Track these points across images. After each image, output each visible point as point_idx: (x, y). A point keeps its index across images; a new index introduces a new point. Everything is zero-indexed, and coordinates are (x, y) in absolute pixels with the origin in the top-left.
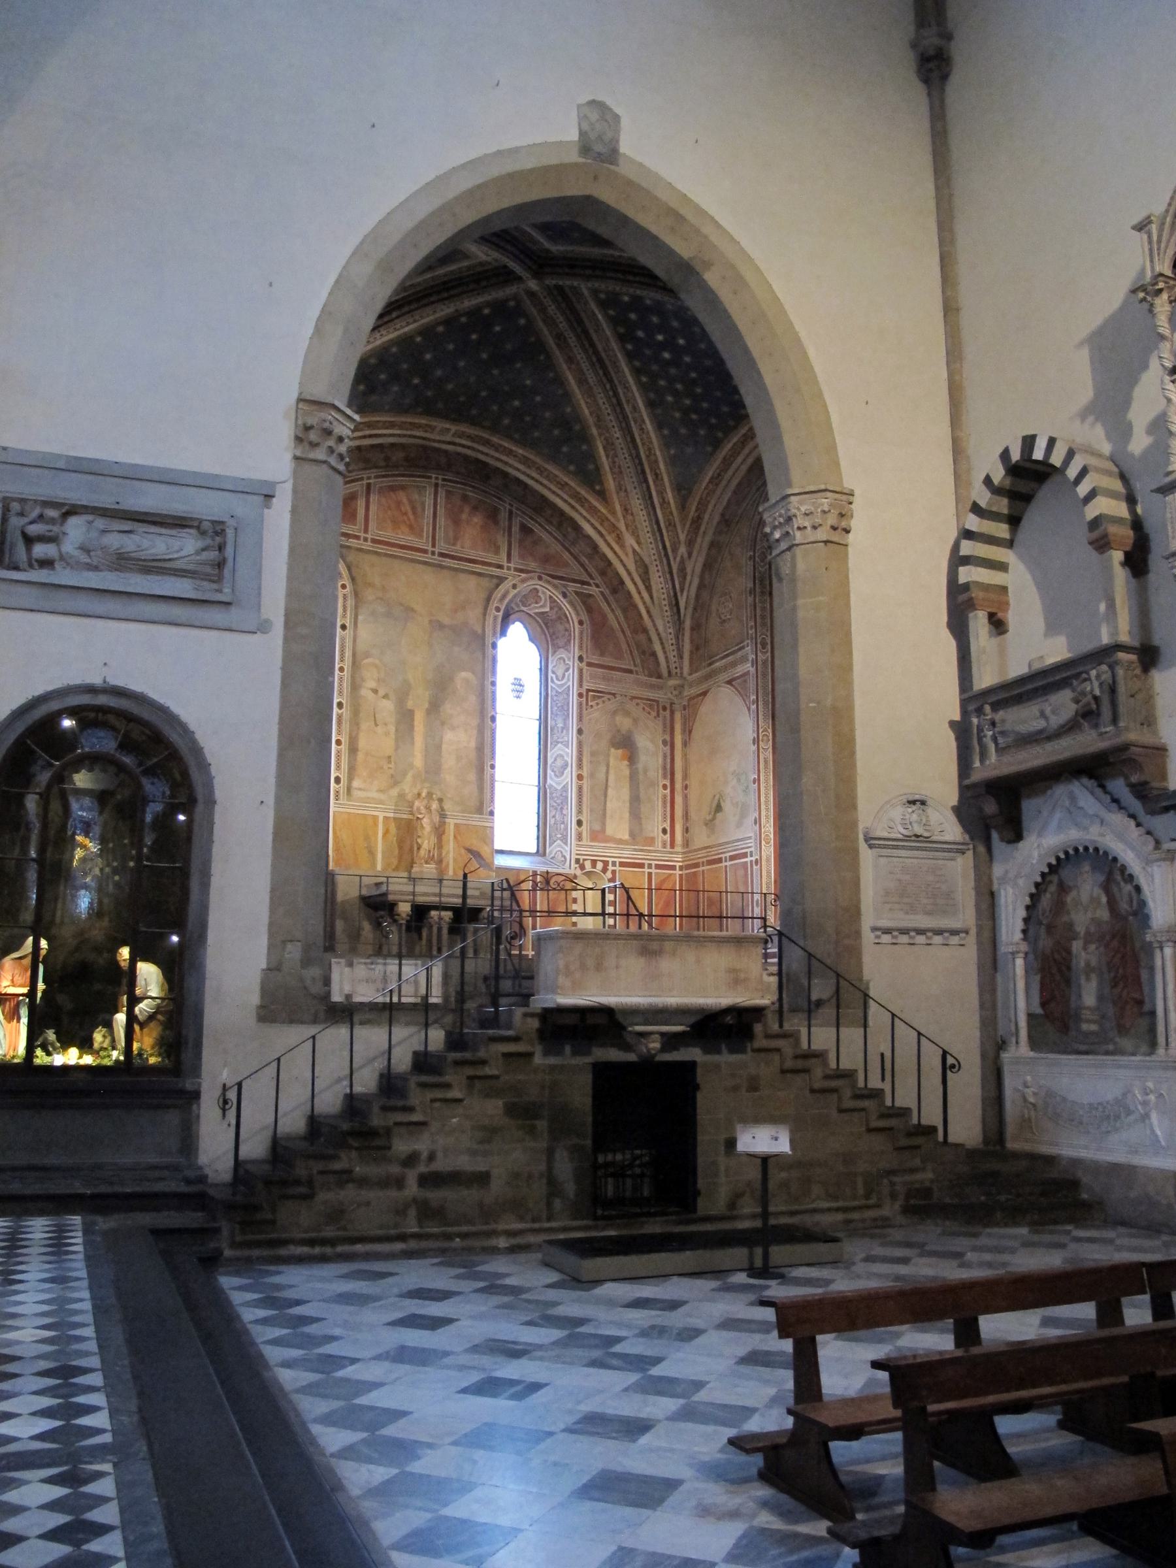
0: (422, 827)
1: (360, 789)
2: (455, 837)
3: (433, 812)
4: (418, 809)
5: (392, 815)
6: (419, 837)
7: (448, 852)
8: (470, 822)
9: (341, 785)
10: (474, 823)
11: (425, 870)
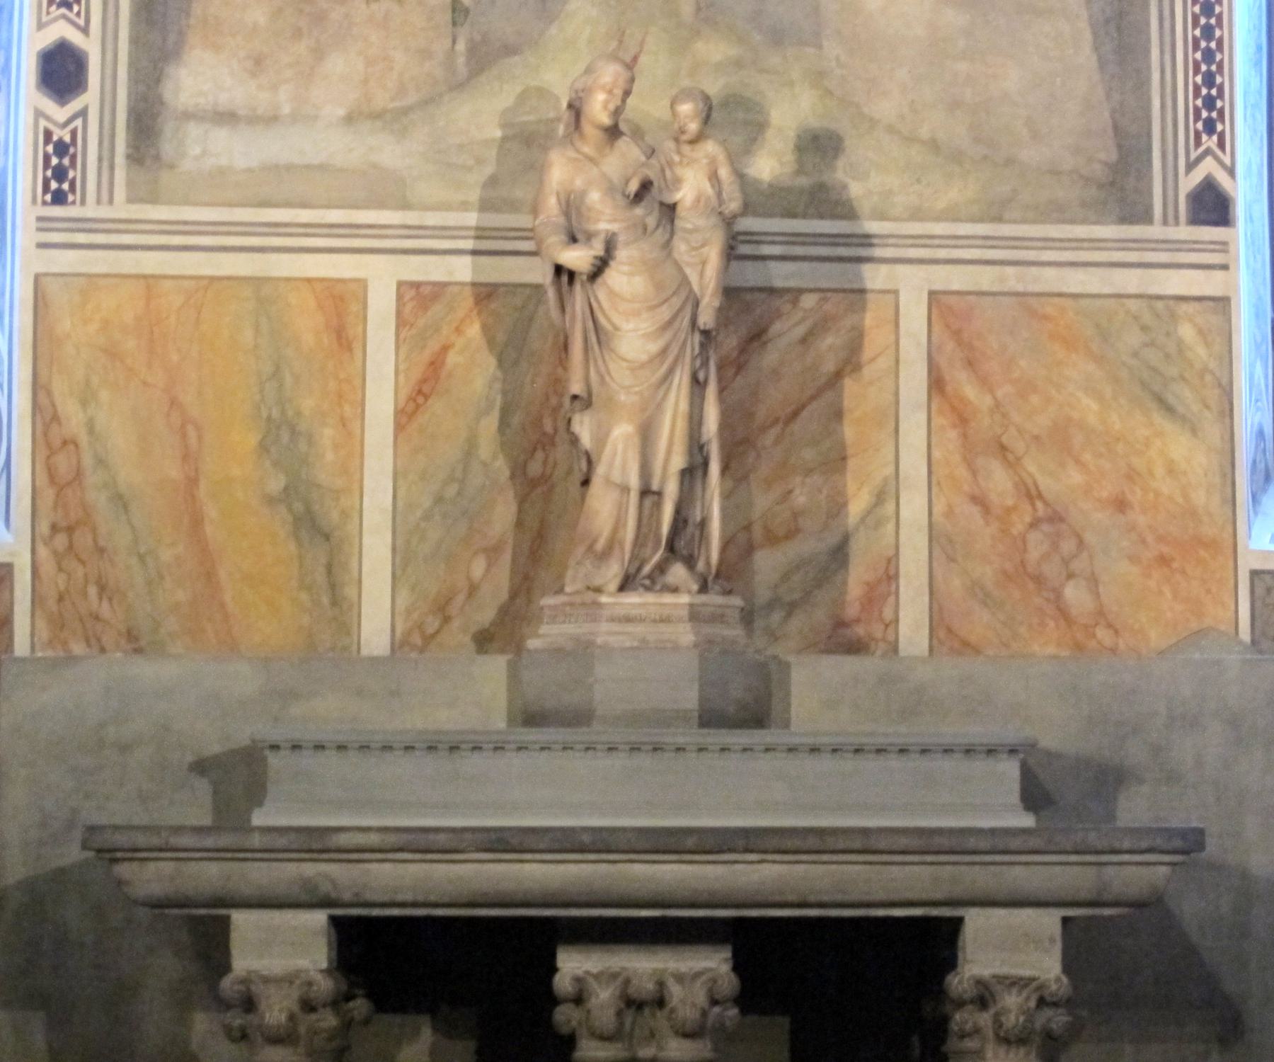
0: (599, 335)
1: (226, 117)
2: (937, 383)
3: (688, 219)
4: (572, 207)
5: (462, 270)
6: (584, 402)
7: (888, 493)
8: (1049, 280)
9: (90, 98)
10: (1077, 281)
11: (605, 633)
